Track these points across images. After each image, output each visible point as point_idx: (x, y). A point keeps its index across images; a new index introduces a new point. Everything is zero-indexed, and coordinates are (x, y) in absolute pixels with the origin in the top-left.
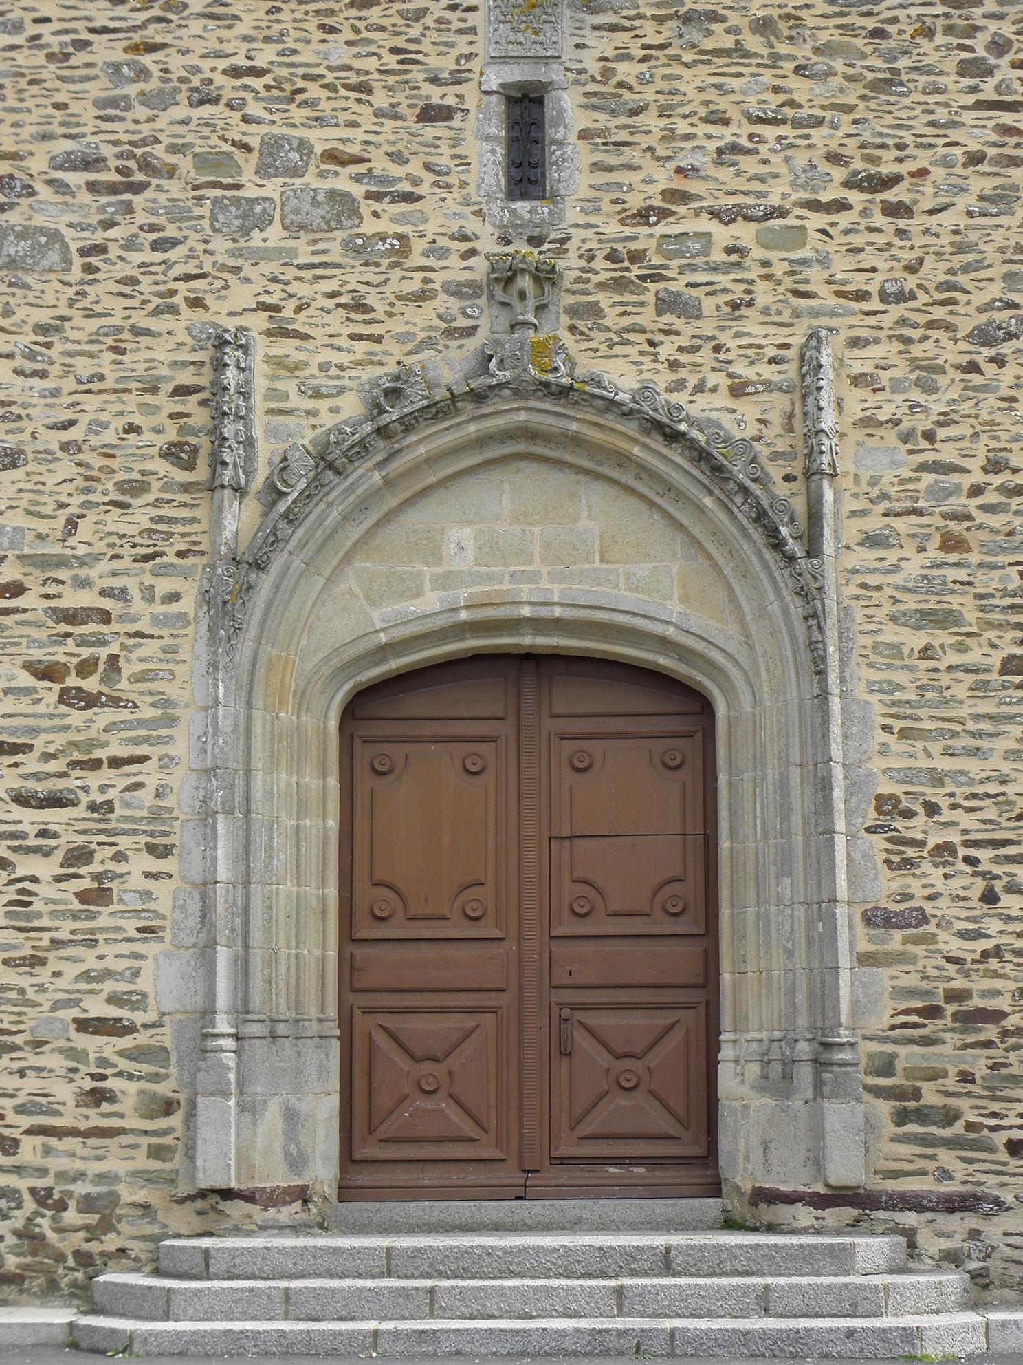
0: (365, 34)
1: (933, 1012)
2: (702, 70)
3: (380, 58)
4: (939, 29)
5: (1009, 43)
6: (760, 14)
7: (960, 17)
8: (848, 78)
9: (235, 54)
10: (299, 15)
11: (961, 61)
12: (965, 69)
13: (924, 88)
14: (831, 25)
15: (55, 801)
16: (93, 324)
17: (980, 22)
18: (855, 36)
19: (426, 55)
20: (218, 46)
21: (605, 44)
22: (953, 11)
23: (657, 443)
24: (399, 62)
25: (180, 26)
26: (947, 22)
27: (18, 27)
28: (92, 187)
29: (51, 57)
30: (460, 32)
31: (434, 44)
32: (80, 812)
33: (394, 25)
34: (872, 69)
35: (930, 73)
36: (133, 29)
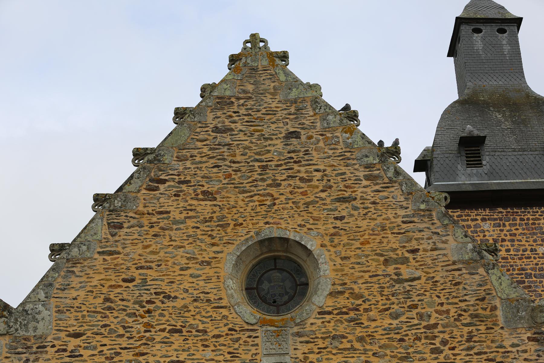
0: (218, 347)
2: (340, 356)
3: (224, 356)
4: (423, 337)
5: (448, 341)
6: (359, 335)
7: (430, 333)
8: (391, 357)
9: (172, 356)
10: (194, 341)
11: (431, 348)
12: (433, 351)
13: (419, 359)
14: (385, 338)
17: (437, 334)
18: (393, 341)
19: (241, 354)
20: (166, 353)
21: (305, 348)
22: (427, 331)
24: (231, 357)
25: (152, 346)
26: (425, 335)
27: (95, 348)
29: (107, 358)
30: (252, 345)
31: (243, 350)
33: (229, 344)
34: (400, 353)
35: (421, 353)
36: (136, 348)
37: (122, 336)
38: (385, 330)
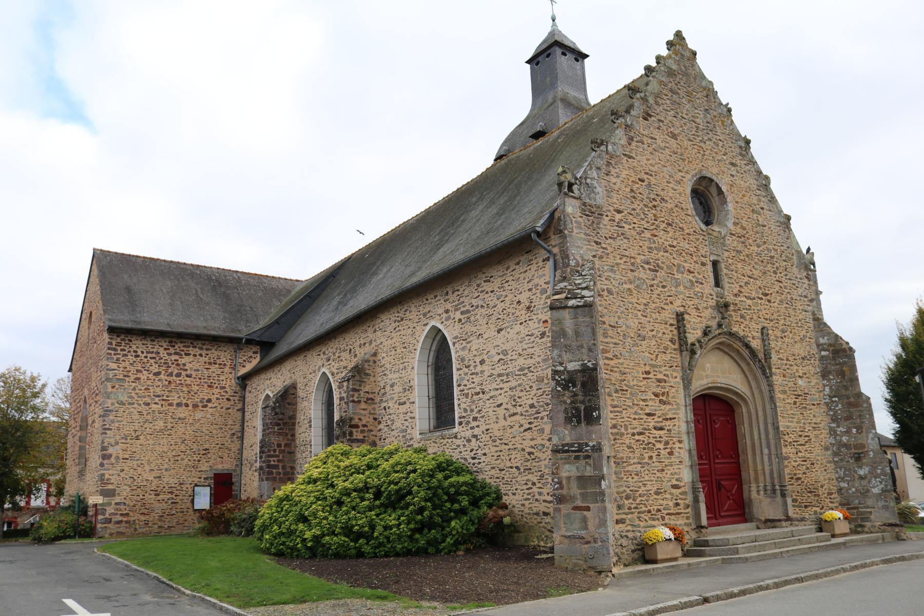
1: (792, 478)
15: (661, 429)
16: (654, 305)
23: (744, 348)
28: (650, 269)
32: (665, 431)
37: (643, 219)
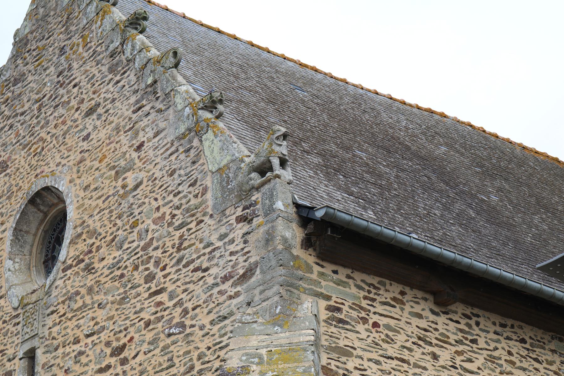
38: (109, 268)
